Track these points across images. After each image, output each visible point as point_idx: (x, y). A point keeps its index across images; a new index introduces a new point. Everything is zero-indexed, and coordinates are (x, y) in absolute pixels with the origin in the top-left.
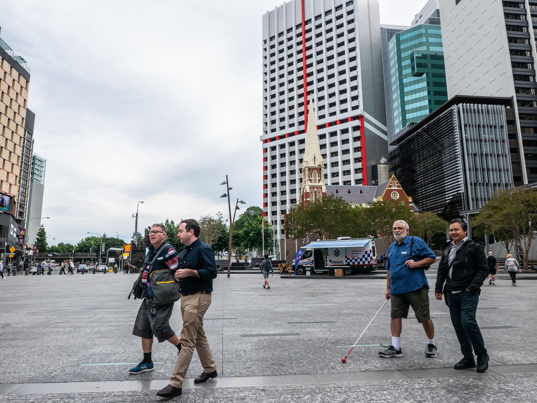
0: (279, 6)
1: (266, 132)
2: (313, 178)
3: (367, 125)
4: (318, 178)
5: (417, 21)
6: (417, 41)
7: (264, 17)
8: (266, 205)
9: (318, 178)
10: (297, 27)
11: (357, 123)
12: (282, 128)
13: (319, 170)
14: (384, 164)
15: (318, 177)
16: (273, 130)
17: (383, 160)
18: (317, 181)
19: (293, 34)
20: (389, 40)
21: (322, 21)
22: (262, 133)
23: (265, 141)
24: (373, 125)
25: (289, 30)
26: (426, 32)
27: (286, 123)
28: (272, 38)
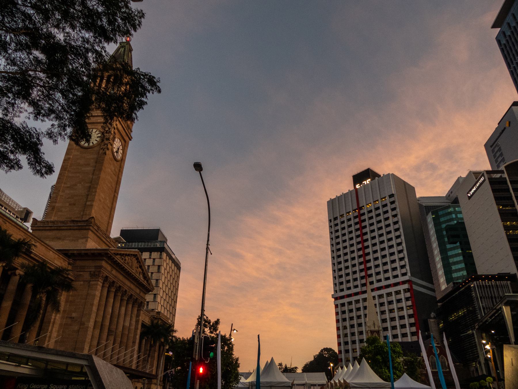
0: (339, 195)
1: (336, 291)
3: (415, 287)
5: (449, 196)
6: (448, 217)
7: (328, 202)
8: (340, 352)
11: (406, 286)
12: (349, 288)
14: (434, 318)
16: (342, 290)
17: (433, 315)
20: (427, 214)
24: (421, 286)
26: (455, 210)
27: (351, 285)
28: (335, 219)
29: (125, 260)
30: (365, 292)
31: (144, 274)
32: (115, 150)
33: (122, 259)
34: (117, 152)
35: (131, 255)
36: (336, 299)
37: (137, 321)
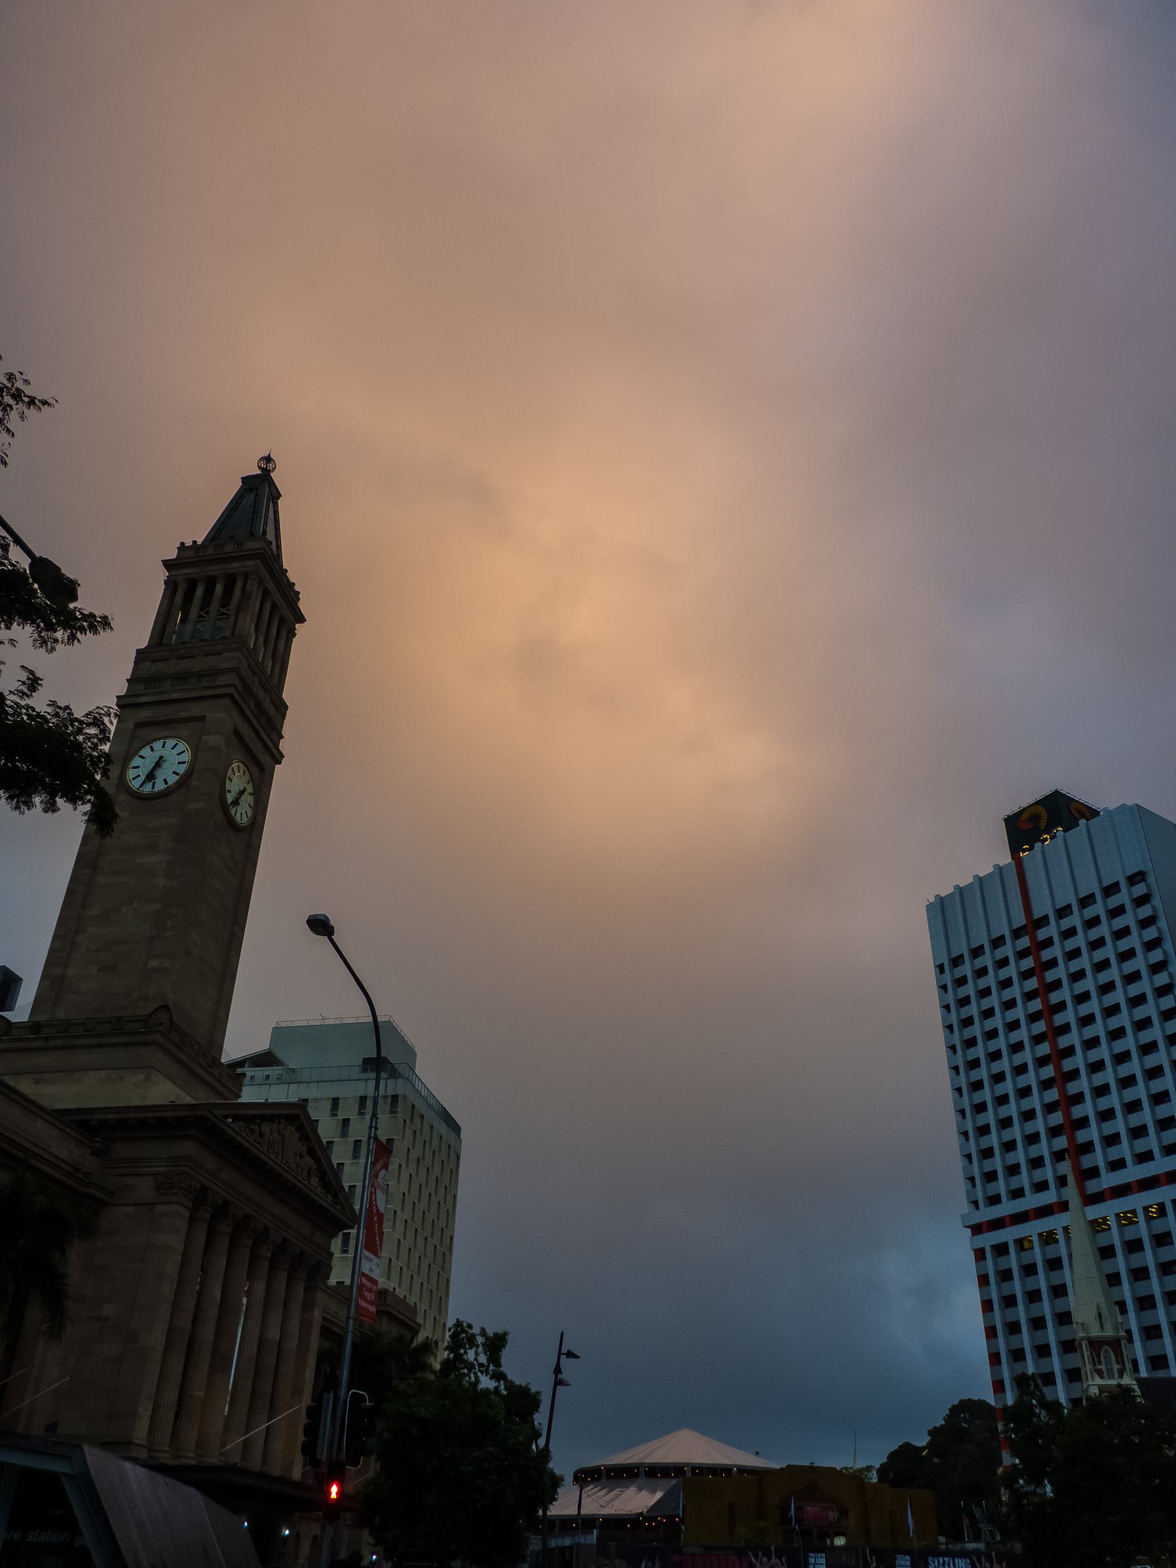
1: (976, 1204)
2: (1103, 1367)
4: (1116, 1367)
7: (930, 908)
9: (1116, 1367)
10: (1017, 934)
12: (1018, 1193)
13: (1115, 1344)
15: (1118, 1363)
16: (994, 1200)
18: (1117, 1375)
19: (1008, 950)
21: (1074, 920)
22: (965, 1207)
23: (977, 1229)
25: (998, 942)
27: (1024, 1179)
28: (957, 961)
29: (261, 1134)
30: (1064, 1206)
31: (322, 1175)
32: (230, 798)
33: (252, 1131)
34: (236, 802)
35: (280, 1116)
36: (977, 1229)
37: (305, 1325)
